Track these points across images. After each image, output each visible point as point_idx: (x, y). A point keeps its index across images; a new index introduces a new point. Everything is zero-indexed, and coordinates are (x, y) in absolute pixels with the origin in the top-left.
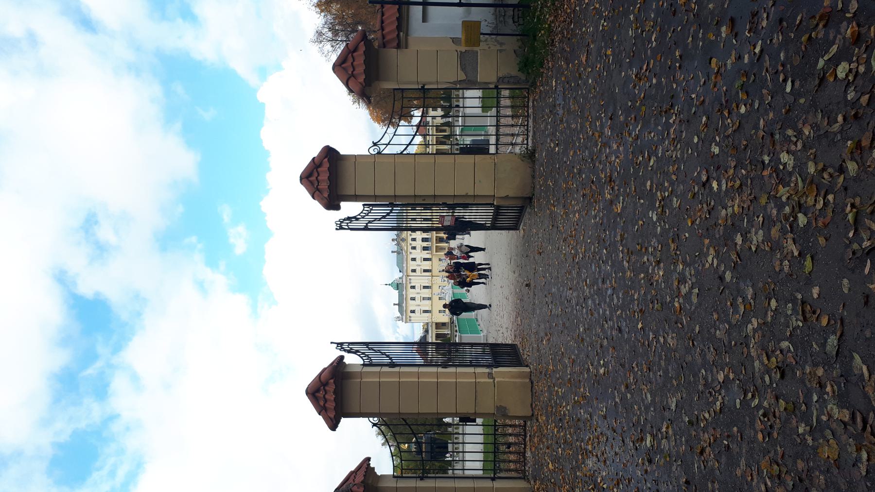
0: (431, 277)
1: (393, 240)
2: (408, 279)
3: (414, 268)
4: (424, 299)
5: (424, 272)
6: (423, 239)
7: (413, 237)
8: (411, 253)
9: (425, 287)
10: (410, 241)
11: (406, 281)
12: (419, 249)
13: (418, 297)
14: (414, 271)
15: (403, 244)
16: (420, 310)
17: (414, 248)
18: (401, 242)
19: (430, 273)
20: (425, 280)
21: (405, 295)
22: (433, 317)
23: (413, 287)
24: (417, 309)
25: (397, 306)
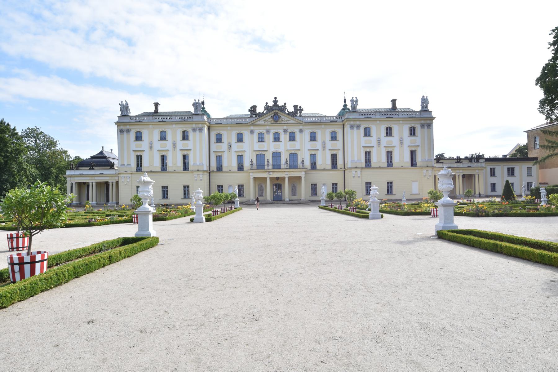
1: (275, 101)
3: (224, 139)
4: (163, 158)
8: (252, 132)
12: (258, 147)
13: (168, 144)
14: (219, 139)
15: (268, 118)
16: (144, 151)
17: (261, 139)
18: (272, 114)
21: (170, 120)
22: (128, 176)
23: (185, 137)
24: (144, 145)
25: (152, 110)
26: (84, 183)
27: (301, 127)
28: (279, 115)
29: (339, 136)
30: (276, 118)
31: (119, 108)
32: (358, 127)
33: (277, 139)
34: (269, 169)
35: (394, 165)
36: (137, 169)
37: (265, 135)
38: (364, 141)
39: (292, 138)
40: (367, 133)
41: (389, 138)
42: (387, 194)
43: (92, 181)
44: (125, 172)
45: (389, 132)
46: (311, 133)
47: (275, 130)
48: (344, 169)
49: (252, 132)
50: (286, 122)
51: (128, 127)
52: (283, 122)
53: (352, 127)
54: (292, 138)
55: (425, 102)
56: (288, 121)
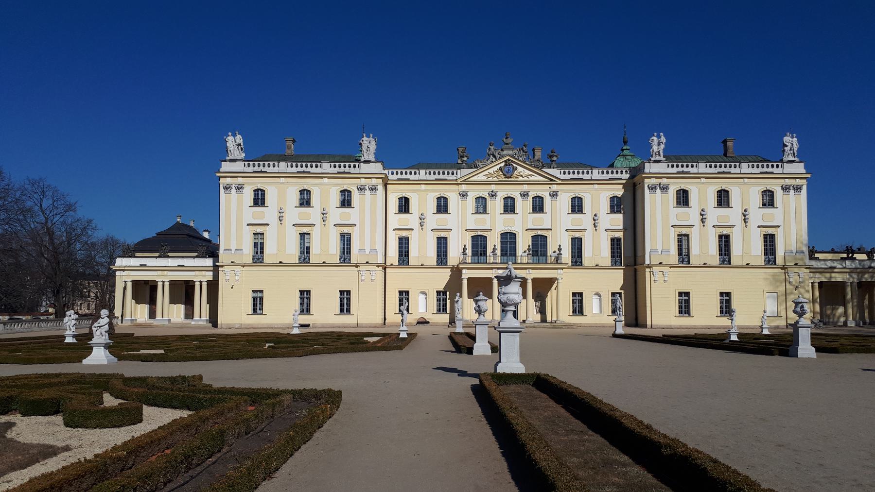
0: (380, 260)
2: (374, 181)
6: (513, 236)
7: (519, 204)
8: (464, 195)
9: (346, 240)
11: (369, 176)
13: (312, 214)
14: (404, 206)
17: (481, 206)
19: (396, 263)
23: (346, 201)
24: (268, 213)
26: (146, 282)
27: (555, 188)
28: (514, 165)
30: (509, 170)
32: (665, 188)
33: (509, 207)
34: (496, 264)
35: (735, 261)
36: (253, 259)
37: (488, 198)
38: (678, 215)
39: (538, 206)
40: (683, 198)
41: (723, 211)
42: (719, 315)
43: (163, 278)
44: (232, 262)
45: (723, 198)
46: (573, 199)
47: (506, 193)
48: (636, 267)
49: (464, 195)
50: (526, 179)
52: (521, 179)
53: (652, 188)
54: (538, 206)
56: (529, 177)
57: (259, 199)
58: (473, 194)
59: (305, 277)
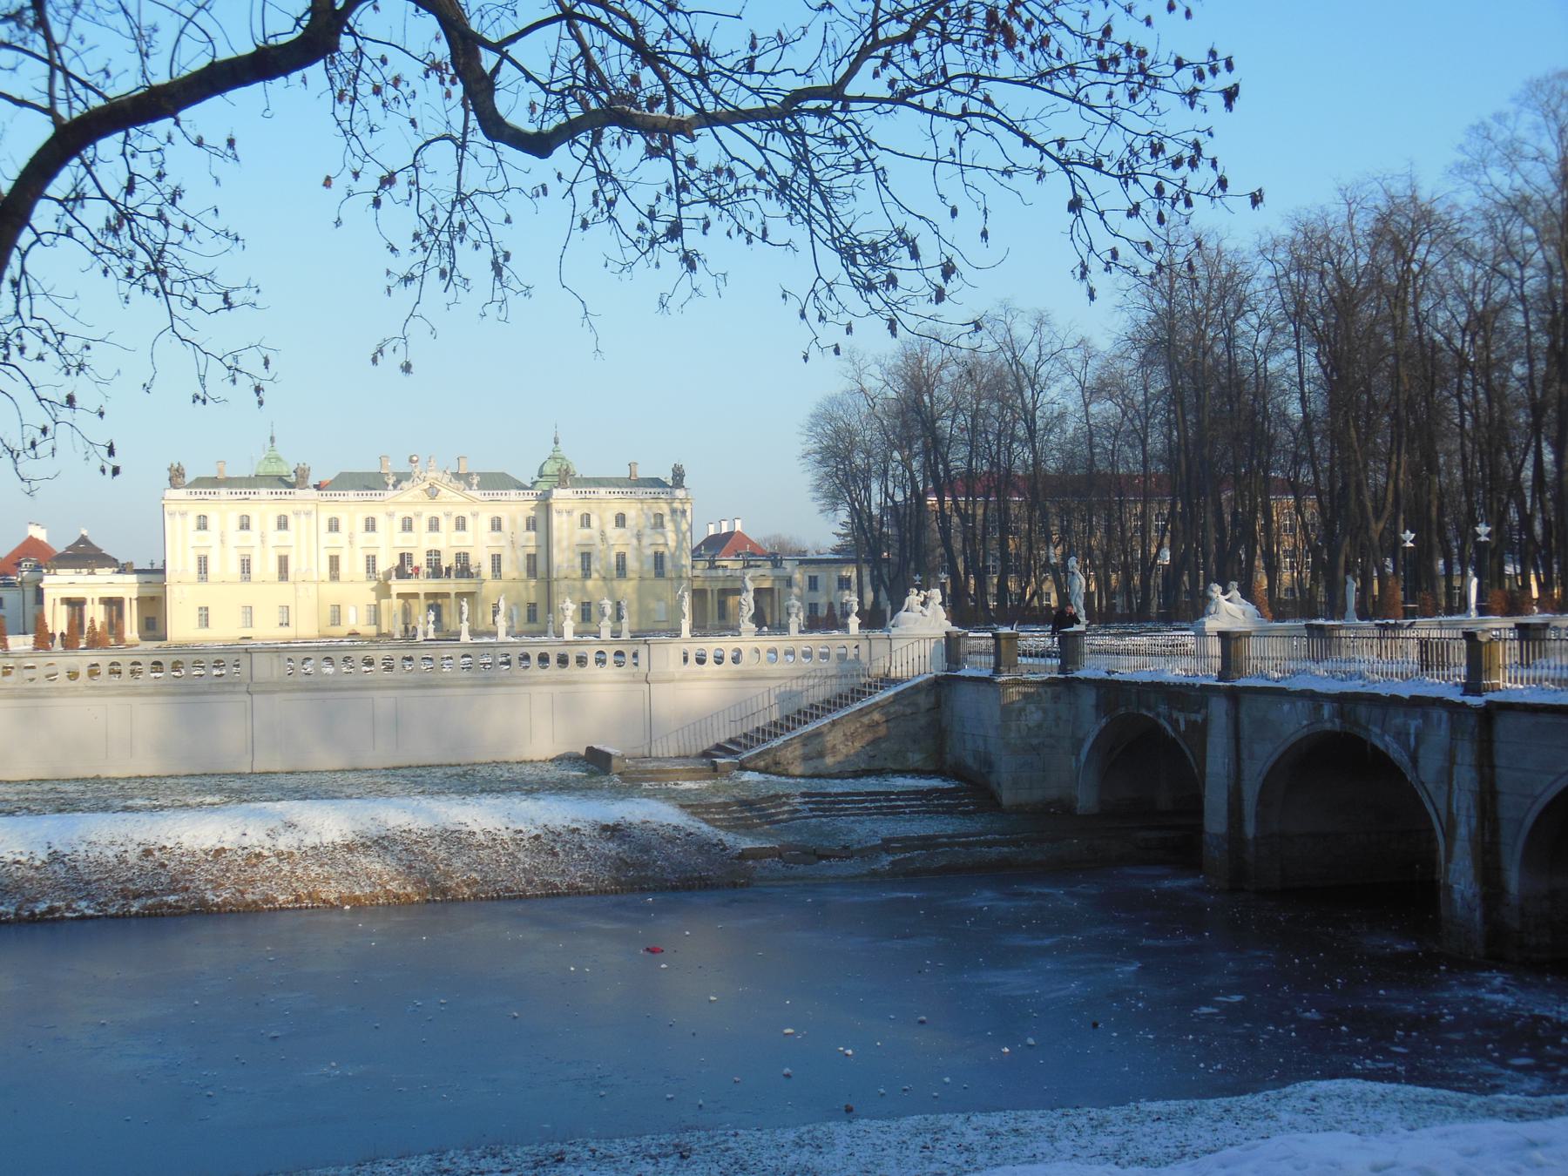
5: (331, 557)
6: (438, 553)
7: (443, 523)
9: (283, 563)
10: (430, 511)
12: (405, 541)
13: (252, 536)
14: (334, 526)
17: (407, 526)
20: (309, 561)
21: (256, 497)
23: (283, 524)
24: (210, 536)
27: (476, 508)
29: (541, 525)
31: (168, 475)
32: (569, 512)
33: (434, 525)
39: (461, 524)
49: (391, 515)
51: (184, 507)
54: (461, 524)
55: (678, 476)
57: (203, 524)
58: (399, 516)
59: (247, 593)
